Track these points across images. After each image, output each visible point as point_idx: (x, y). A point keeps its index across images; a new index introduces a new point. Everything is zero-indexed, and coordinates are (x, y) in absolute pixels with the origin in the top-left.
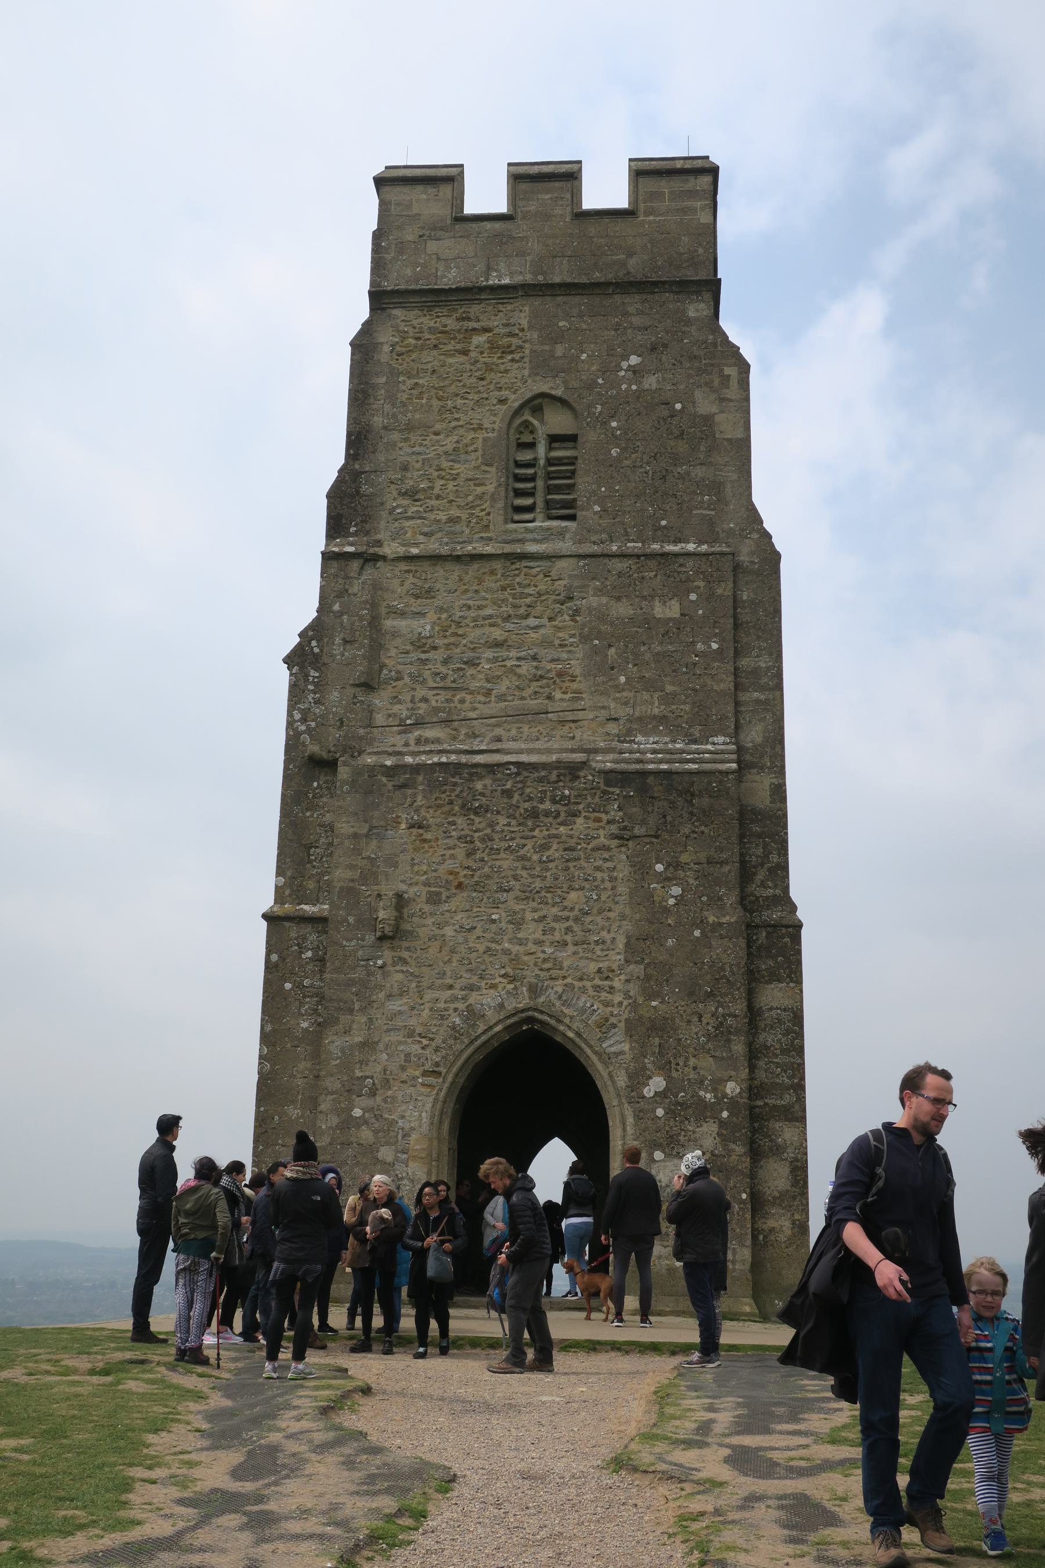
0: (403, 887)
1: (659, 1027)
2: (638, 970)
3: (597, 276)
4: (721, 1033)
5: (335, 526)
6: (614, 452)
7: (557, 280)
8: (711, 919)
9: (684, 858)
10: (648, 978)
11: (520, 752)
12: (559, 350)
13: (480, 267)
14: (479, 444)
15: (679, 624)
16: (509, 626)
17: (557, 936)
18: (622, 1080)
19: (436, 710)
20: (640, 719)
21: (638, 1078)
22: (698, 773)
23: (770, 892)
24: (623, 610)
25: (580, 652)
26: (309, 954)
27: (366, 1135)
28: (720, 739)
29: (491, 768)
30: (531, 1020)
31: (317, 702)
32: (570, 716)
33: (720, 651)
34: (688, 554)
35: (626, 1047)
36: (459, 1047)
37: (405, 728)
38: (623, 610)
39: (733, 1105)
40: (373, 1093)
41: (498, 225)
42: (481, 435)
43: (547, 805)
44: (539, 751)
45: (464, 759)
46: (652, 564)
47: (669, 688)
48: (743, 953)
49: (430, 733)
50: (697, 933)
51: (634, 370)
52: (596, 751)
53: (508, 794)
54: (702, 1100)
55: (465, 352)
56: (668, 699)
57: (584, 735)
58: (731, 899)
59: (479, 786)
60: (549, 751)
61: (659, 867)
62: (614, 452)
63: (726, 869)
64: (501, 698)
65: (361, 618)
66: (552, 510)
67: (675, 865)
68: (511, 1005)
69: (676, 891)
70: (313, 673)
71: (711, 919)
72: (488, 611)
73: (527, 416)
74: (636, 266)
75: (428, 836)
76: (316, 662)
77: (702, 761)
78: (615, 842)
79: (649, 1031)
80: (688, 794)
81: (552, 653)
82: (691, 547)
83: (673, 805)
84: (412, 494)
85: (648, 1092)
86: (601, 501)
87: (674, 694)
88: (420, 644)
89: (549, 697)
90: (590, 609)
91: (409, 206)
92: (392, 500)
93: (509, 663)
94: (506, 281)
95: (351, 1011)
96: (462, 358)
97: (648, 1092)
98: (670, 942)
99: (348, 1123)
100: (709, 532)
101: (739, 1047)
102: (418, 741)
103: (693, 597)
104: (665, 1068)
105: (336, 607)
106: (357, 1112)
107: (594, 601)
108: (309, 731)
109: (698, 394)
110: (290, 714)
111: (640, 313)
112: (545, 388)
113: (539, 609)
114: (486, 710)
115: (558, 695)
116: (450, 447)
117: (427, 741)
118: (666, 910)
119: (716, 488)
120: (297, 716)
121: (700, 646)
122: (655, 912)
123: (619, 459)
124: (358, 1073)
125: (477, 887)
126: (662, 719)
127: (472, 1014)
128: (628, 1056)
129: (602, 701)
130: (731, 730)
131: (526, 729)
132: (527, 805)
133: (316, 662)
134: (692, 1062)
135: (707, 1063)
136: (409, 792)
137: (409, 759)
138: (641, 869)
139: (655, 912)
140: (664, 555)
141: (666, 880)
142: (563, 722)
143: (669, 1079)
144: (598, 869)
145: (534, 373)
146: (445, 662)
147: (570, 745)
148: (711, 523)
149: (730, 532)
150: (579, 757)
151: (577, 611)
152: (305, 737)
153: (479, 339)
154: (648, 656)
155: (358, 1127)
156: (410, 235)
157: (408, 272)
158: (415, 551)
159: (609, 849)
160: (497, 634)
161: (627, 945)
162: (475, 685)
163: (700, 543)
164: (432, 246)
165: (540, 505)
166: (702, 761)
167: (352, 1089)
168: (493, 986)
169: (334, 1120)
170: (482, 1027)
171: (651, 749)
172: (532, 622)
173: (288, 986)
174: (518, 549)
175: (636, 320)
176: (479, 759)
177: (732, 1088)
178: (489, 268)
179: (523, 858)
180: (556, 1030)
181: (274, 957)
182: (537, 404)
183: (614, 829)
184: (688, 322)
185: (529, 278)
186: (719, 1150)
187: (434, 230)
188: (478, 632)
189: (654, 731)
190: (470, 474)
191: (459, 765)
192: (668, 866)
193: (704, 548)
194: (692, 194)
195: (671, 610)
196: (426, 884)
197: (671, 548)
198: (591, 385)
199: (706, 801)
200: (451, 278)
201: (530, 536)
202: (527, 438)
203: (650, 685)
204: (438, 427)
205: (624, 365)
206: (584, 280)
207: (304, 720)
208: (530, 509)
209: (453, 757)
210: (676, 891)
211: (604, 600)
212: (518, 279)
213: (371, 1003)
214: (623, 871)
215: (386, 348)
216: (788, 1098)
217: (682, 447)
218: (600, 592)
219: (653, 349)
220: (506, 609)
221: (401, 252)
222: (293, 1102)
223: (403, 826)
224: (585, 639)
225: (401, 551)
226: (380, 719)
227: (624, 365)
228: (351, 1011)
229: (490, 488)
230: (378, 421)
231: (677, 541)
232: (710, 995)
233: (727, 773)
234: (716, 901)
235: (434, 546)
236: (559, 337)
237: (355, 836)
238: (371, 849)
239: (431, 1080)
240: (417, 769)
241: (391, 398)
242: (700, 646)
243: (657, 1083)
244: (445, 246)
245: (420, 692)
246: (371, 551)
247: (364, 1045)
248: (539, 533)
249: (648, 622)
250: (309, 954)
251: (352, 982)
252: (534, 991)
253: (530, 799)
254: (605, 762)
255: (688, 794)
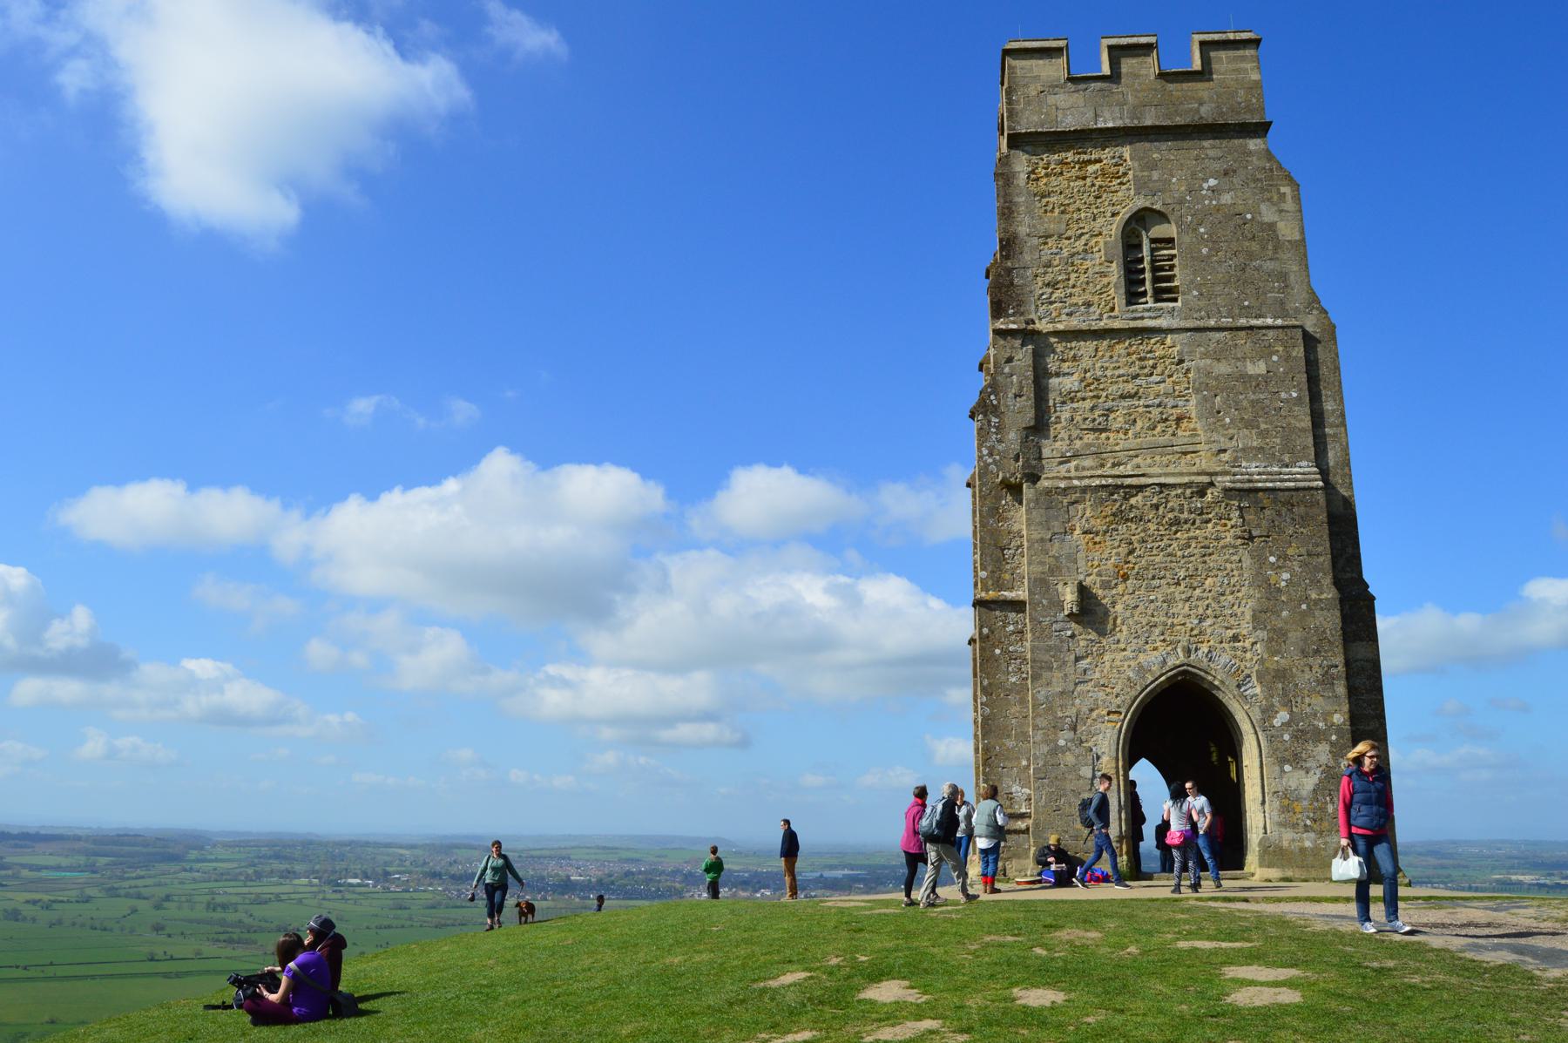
0: (1081, 577)
1: (1282, 675)
2: (1263, 634)
3: (1179, 120)
4: (1327, 680)
5: (998, 310)
6: (1205, 251)
7: (1148, 123)
8: (1314, 596)
9: (1290, 552)
10: (1271, 640)
11: (1160, 475)
12: (1155, 175)
13: (1090, 114)
14: (1101, 245)
15: (1266, 379)
16: (1138, 381)
17: (1201, 611)
18: (1256, 714)
19: (1089, 445)
20: (1243, 450)
21: (1268, 712)
22: (1297, 489)
23: (1348, 575)
24: (1223, 368)
25: (1193, 401)
26: (1011, 628)
27: (1069, 758)
28: (1304, 463)
29: (1141, 488)
30: (1185, 672)
31: (1000, 441)
32: (1191, 448)
33: (1299, 398)
34: (1269, 327)
35: (1258, 690)
36: (1134, 693)
37: (1065, 460)
38: (1223, 368)
39: (1339, 730)
40: (1074, 729)
41: (1099, 85)
42: (1099, 239)
43: (1186, 515)
44: (1173, 475)
45: (1119, 481)
46: (1243, 333)
47: (1263, 426)
48: (1338, 621)
49: (1088, 462)
50: (1304, 607)
51: (1212, 190)
52: (1216, 474)
53: (1156, 507)
54: (1316, 728)
55: (1084, 178)
56: (1263, 434)
57: (1204, 462)
58: (1327, 580)
59: (1133, 501)
60: (1181, 474)
61: (1272, 559)
62: (1205, 251)
63: (1321, 559)
64: (1136, 436)
65: (1026, 378)
66: (1159, 295)
67: (1284, 557)
68: (1171, 662)
69: (1286, 576)
70: (994, 420)
71: (1314, 596)
72: (1121, 371)
73: (1133, 225)
74: (1207, 113)
75: (1097, 539)
76: (995, 410)
77: (1296, 480)
78: (1239, 541)
79: (1277, 678)
80: (1290, 505)
81: (1170, 402)
82: (1269, 321)
83: (1279, 514)
84: (1053, 285)
85: (1277, 722)
86: (1199, 287)
87: (1267, 431)
88: (1071, 397)
89: (1174, 435)
90: (1198, 370)
91: (1031, 70)
92: (1038, 288)
93: (1141, 410)
94: (1110, 125)
95: (1051, 669)
96: (1081, 183)
97: (1277, 722)
98: (1285, 613)
99: (1055, 750)
100: (1281, 309)
101: (1341, 689)
102: (1077, 469)
103: (1275, 358)
104: (1288, 704)
105: (1007, 370)
106: (1062, 742)
107: (1202, 363)
108: (995, 462)
109: (1263, 207)
110: (979, 450)
111: (1214, 147)
112: (1148, 204)
113: (1159, 370)
114: (1127, 446)
115: (1180, 433)
116: (1081, 249)
117: (1084, 469)
118: (1279, 590)
119: (1283, 277)
120: (985, 452)
121: (1283, 395)
122: (1272, 591)
123: (1209, 256)
124: (1060, 714)
125: (1138, 576)
126: (1260, 449)
127: (1141, 670)
128: (1261, 697)
129: (1215, 436)
130: (1312, 456)
131: (1157, 458)
132: (1171, 515)
133: (995, 410)
134: (1307, 700)
135: (1318, 703)
136: (1080, 507)
137: (1076, 482)
138: (1260, 560)
139: (1272, 591)
140: (1251, 328)
141: (1277, 568)
142: (1185, 453)
143: (1291, 712)
144: (1227, 561)
145: (1138, 193)
146: (1092, 409)
147: (1194, 469)
148: (1282, 303)
149: (1297, 310)
150: (1206, 479)
151: (1188, 370)
152: (993, 468)
153: (1091, 168)
154: (1245, 403)
155: (1063, 753)
156: (1033, 91)
157: (1035, 118)
158: (1061, 327)
159: (1235, 547)
160: (1130, 388)
161: (1254, 617)
162: (1116, 426)
163: (1276, 318)
164: (1051, 99)
165: (1150, 293)
166: (1296, 480)
167: (1056, 727)
168: (1155, 649)
169: (1045, 749)
170: (1151, 679)
171: (1254, 470)
172: (1155, 378)
173: (998, 651)
174: (1139, 324)
175: (1211, 153)
176: (1128, 481)
177: (1338, 718)
178: (1096, 115)
179: (1169, 555)
180: (1203, 679)
181: (985, 631)
182: (1142, 218)
183: (1238, 531)
184: (1250, 153)
185: (1128, 123)
186: (1331, 763)
187: (1053, 87)
188: (1115, 387)
189: (1255, 458)
190: (1097, 269)
191: (1118, 487)
192: (1279, 557)
193: (1279, 322)
194: (1243, 59)
195: (1259, 368)
196: (1099, 574)
197: (1254, 322)
198: (1181, 202)
199: (1302, 509)
200: (1069, 123)
201: (1146, 314)
202: (1135, 241)
203: (1250, 425)
204: (1069, 233)
205: (1205, 186)
206: (1168, 123)
207: (991, 454)
208: (1144, 294)
209: (1110, 481)
210: (1286, 576)
211: (1208, 361)
212: (1119, 123)
213: (1064, 663)
214: (1247, 562)
215: (1024, 176)
216: (1373, 725)
217: (1255, 246)
218: (1205, 355)
219: (1226, 174)
220: (1135, 369)
221: (1028, 103)
222: (1009, 736)
223: (1078, 531)
224: (1197, 391)
225: (1050, 328)
226: (1046, 452)
227: (1205, 186)
228: (1051, 669)
229: (1114, 279)
230: (1023, 230)
231: (1257, 317)
232: (1317, 652)
233: (1317, 489)
234: (1316, 583)
235: (1075, 323)
236: (1153, 166)
237: (1042, 540)
238: (1055, 549)
239: (1113, 717)
240: (1084, 490)
241: (1030, 212)
242: (1283, 395)
243: (1282, 716)
244: (1061, 99)
245: (1075, 433)
246: (1030, 327)
247: (1062, 693)
248: (1150, 313)
249: (1244, 378)
250: (1011, 628)
251: (1050, 648)
252: (1188, 652)
253: (1172, 510)
254: (1224, 481)
255: (1290, 505)
